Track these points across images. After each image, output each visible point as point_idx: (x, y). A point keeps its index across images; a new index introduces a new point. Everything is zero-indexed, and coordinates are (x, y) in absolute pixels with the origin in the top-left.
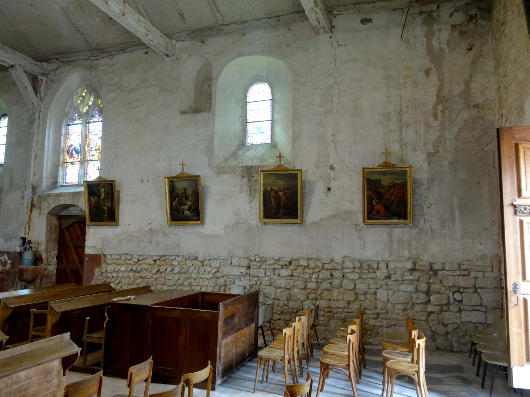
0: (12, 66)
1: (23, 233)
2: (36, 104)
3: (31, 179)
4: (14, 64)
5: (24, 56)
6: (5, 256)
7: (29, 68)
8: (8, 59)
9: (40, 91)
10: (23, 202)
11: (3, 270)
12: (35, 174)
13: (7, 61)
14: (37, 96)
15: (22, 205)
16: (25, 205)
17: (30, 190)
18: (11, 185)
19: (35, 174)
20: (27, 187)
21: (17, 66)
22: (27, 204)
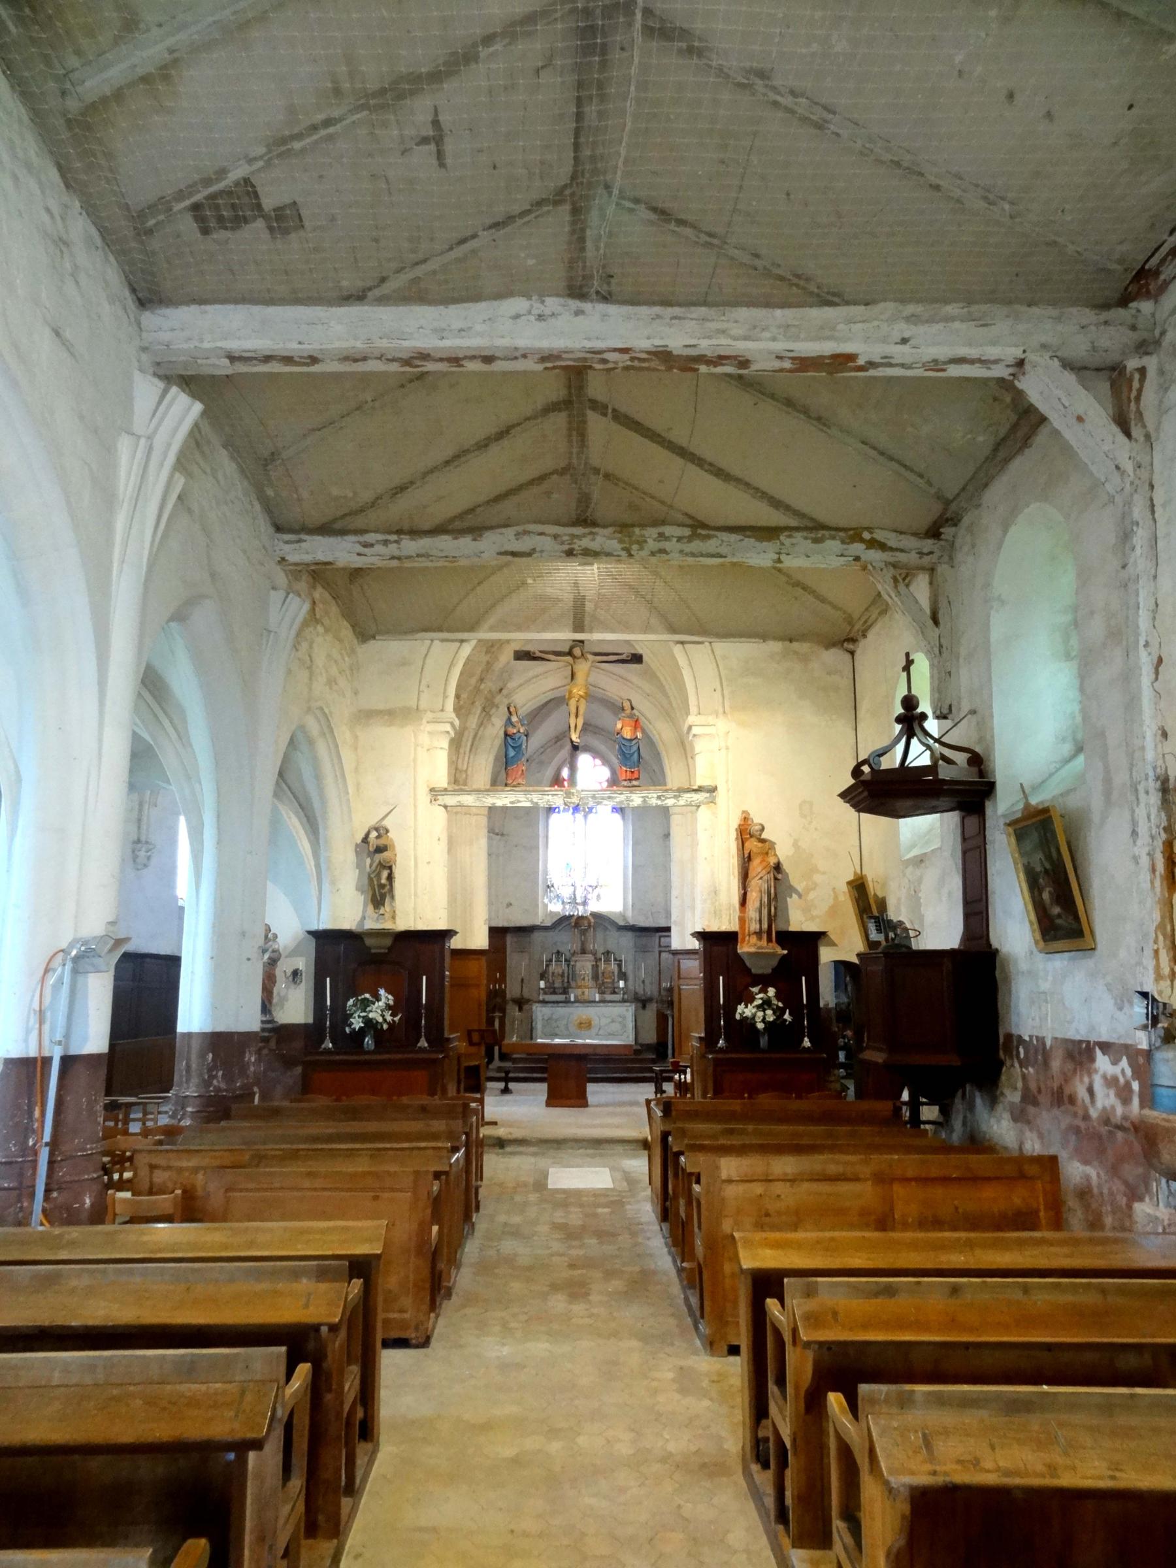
0: (1021, 363)
1: (1151, 975)
2: (1128, 466)
3: (1150, 755)
4: (1018, 353)
5: (1053, 312)
6: (1124, 1062)
7: (1079, 348)
8: (993, 343)
9: (1140, 414)
10: (1136, 851)
11: (1125, 1118)
12: (1165, 735)
13: (992, 352)
14: (1128, 434)
15: (1136, 859)
16: (1145, 861)
17: (1155, 799)
18: (1108, 793)
19: (1165, 735)
20: (1141, 788)
21: (1031, 357)
22: (1150, 855)
